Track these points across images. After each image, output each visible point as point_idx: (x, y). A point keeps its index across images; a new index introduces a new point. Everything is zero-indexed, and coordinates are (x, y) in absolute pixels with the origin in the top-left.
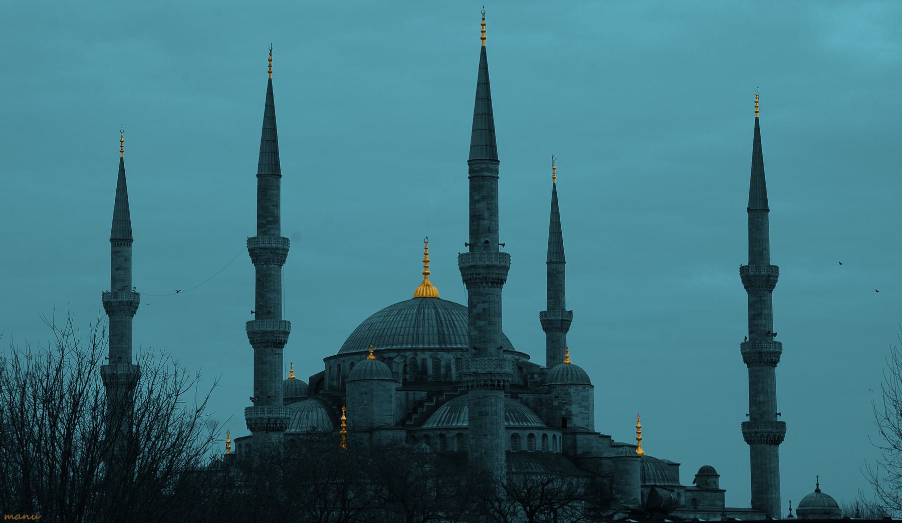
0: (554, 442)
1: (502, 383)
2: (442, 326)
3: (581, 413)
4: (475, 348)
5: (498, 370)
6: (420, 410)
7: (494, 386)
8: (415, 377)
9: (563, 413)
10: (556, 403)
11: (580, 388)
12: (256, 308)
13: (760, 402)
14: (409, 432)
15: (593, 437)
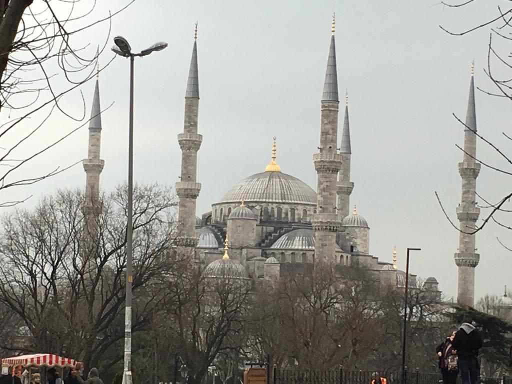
0: (347, 260)
1: (335, 228)
2: (283, 189)
3: (361, 243)
4: (321, 207)
5: (334, 220)
6: (269, 238)
7: (330, 229)
8: (266, 219)
9: (352, 243)
10: (347, 237)
11: (362, 229)
12: (182, 175)
13: (466, 242)
14: (263, 250)
15: (368, 258)
